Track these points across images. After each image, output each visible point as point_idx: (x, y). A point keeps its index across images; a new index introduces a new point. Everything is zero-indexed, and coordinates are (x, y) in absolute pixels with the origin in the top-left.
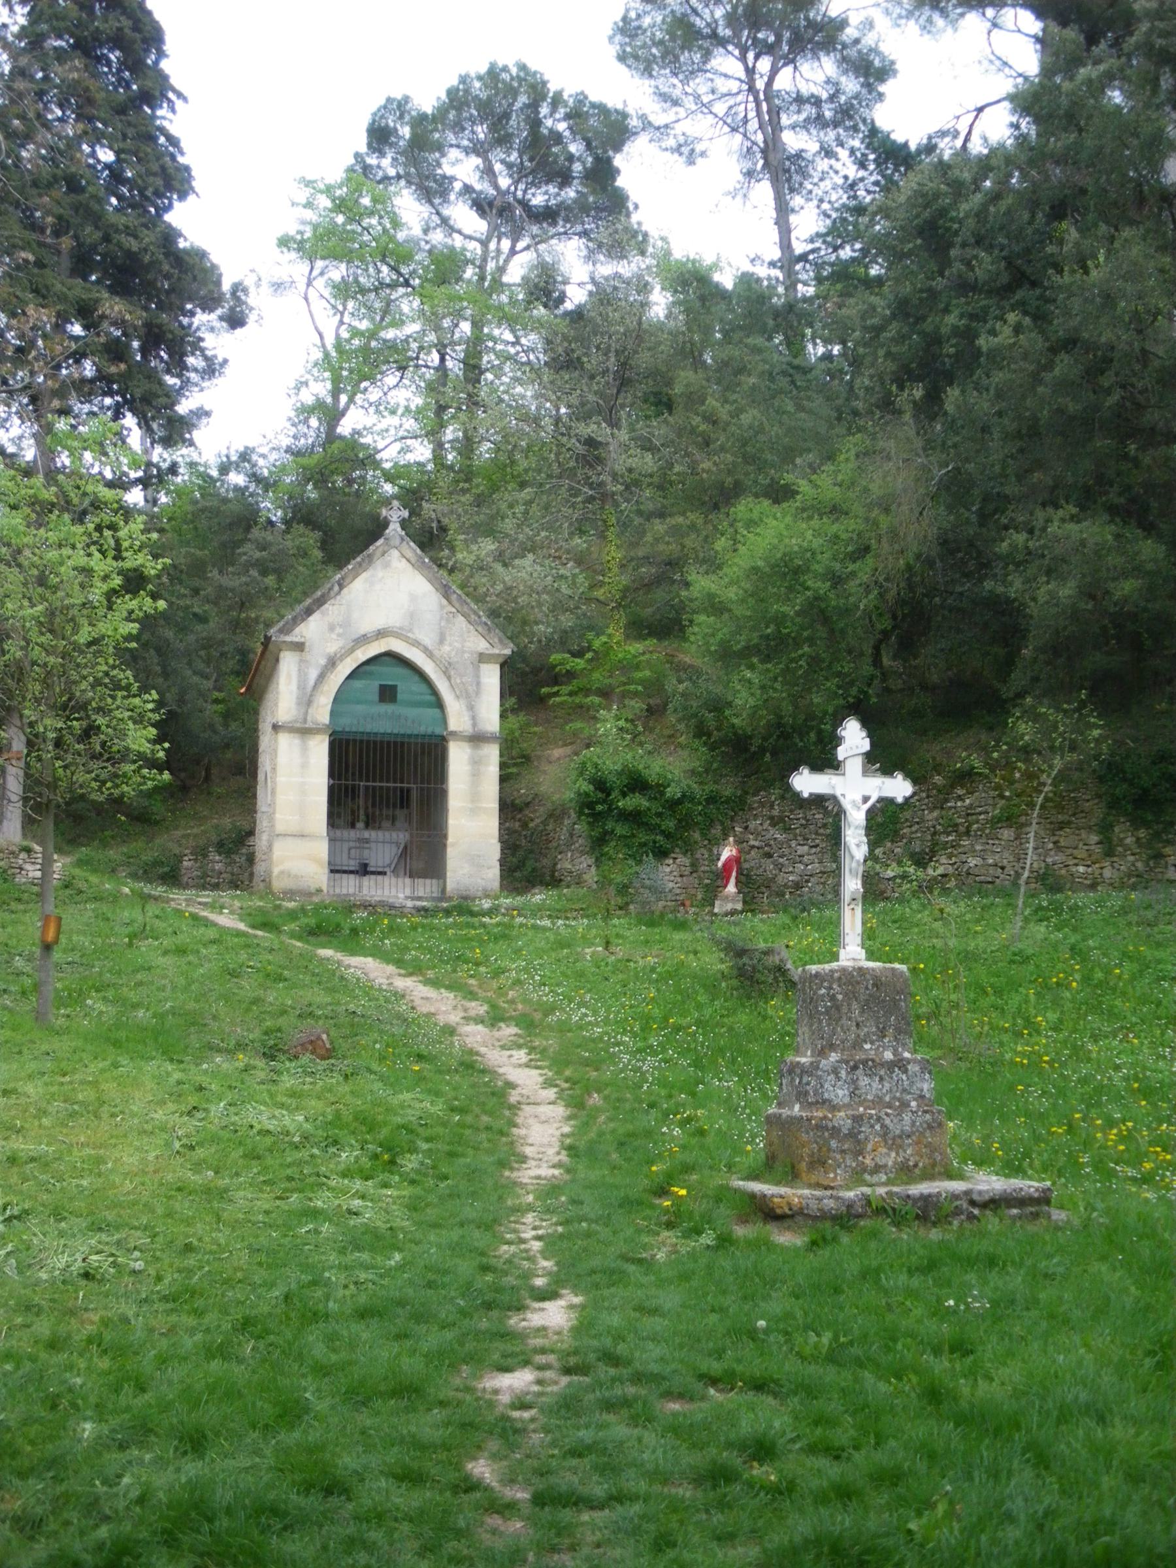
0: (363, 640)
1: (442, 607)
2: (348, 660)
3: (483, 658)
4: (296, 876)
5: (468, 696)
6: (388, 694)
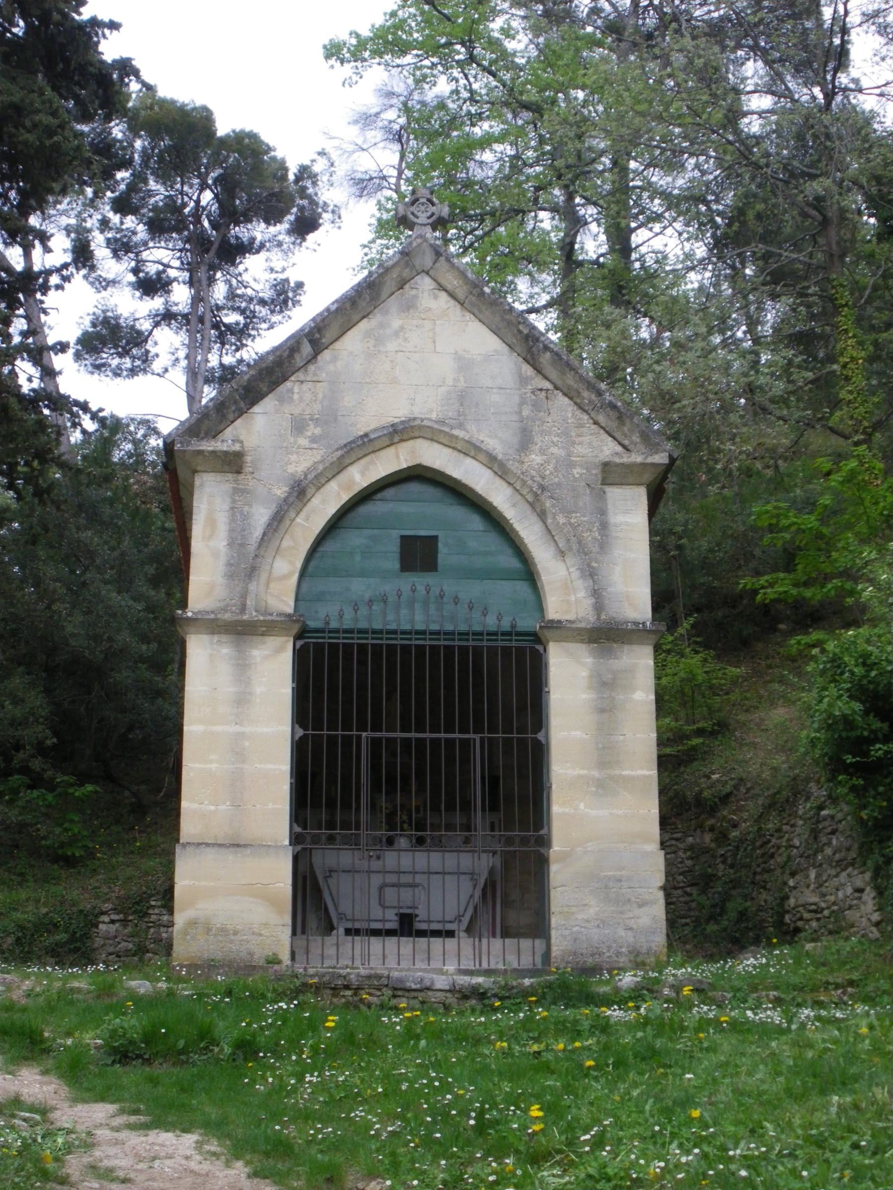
0: (363, 446)
1: (523, 380)
2: (333, 485)
3: (611, 474)
4: (223, 931)
5: (583, 550)
6: (419, 554)
